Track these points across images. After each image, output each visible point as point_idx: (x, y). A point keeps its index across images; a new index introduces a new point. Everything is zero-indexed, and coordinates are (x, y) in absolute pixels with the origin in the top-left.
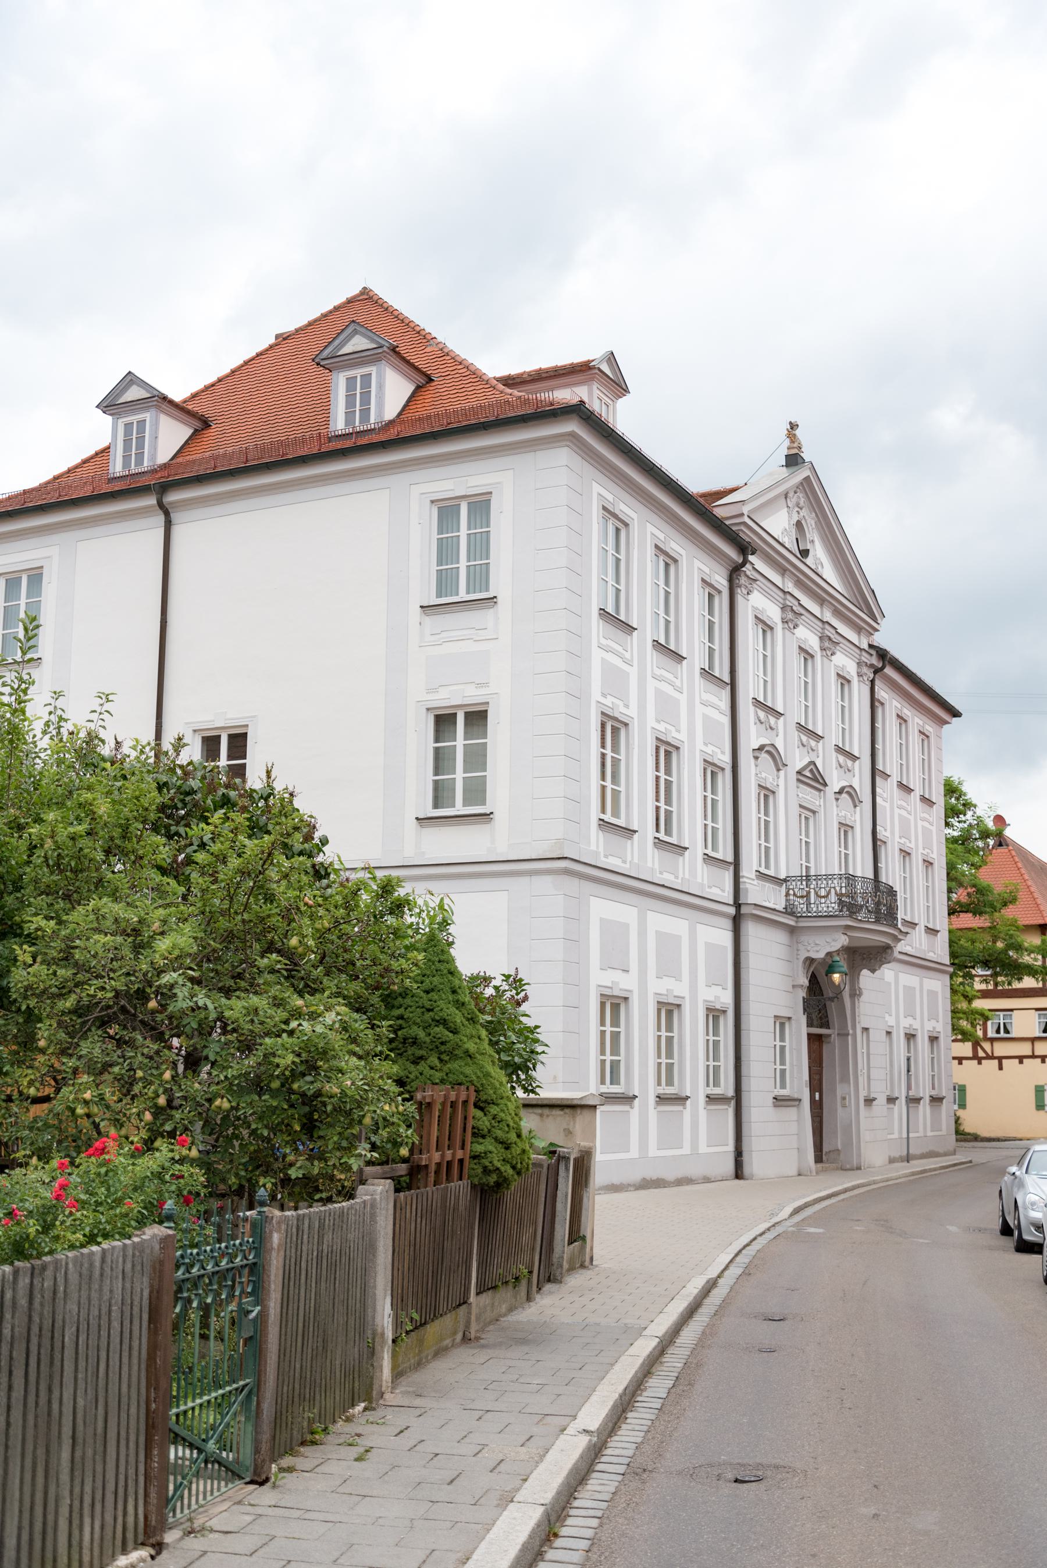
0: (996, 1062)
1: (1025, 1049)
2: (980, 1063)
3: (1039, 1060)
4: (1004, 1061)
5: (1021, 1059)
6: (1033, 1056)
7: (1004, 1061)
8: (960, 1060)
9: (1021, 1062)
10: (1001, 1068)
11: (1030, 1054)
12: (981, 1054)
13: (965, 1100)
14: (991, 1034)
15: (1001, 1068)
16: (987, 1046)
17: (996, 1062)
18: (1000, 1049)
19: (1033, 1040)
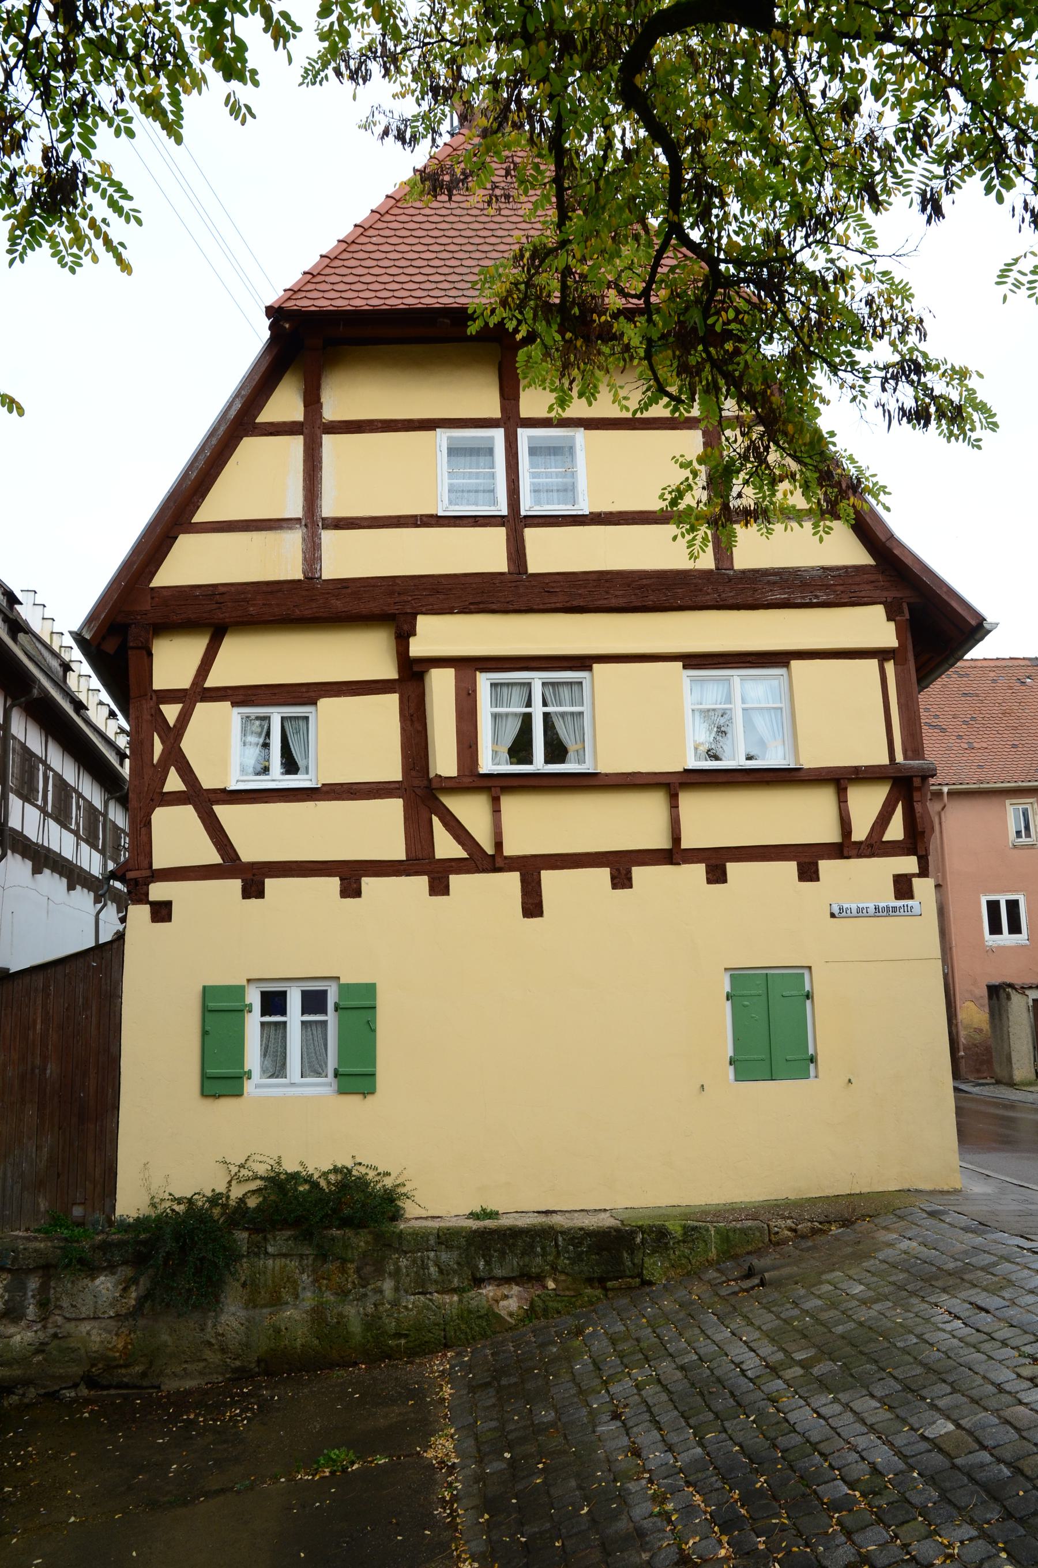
0: (512, 880)
1: (639, 823)
2: (439, 887)
3: (699, 870)
4: (548, 878)
5: (620, 867)
6: (673, 854)
7: (548, 878)
8: (351, 876)
9: (621, 880)
10: (532, 906)
11: (661, 842)
12: (446, 846)
13: (369, 1053)
14: (487, 764)
15: (532, 906)
16: (471, 811)
17: (512, 880)
18: (532, 825)
19: (674, 785)
